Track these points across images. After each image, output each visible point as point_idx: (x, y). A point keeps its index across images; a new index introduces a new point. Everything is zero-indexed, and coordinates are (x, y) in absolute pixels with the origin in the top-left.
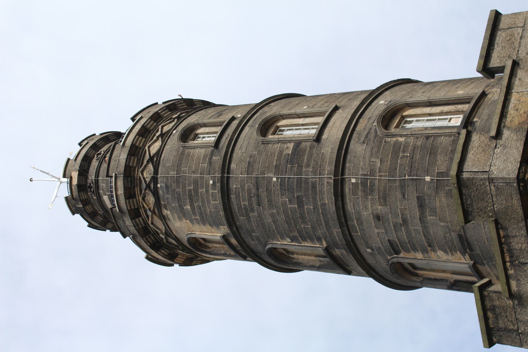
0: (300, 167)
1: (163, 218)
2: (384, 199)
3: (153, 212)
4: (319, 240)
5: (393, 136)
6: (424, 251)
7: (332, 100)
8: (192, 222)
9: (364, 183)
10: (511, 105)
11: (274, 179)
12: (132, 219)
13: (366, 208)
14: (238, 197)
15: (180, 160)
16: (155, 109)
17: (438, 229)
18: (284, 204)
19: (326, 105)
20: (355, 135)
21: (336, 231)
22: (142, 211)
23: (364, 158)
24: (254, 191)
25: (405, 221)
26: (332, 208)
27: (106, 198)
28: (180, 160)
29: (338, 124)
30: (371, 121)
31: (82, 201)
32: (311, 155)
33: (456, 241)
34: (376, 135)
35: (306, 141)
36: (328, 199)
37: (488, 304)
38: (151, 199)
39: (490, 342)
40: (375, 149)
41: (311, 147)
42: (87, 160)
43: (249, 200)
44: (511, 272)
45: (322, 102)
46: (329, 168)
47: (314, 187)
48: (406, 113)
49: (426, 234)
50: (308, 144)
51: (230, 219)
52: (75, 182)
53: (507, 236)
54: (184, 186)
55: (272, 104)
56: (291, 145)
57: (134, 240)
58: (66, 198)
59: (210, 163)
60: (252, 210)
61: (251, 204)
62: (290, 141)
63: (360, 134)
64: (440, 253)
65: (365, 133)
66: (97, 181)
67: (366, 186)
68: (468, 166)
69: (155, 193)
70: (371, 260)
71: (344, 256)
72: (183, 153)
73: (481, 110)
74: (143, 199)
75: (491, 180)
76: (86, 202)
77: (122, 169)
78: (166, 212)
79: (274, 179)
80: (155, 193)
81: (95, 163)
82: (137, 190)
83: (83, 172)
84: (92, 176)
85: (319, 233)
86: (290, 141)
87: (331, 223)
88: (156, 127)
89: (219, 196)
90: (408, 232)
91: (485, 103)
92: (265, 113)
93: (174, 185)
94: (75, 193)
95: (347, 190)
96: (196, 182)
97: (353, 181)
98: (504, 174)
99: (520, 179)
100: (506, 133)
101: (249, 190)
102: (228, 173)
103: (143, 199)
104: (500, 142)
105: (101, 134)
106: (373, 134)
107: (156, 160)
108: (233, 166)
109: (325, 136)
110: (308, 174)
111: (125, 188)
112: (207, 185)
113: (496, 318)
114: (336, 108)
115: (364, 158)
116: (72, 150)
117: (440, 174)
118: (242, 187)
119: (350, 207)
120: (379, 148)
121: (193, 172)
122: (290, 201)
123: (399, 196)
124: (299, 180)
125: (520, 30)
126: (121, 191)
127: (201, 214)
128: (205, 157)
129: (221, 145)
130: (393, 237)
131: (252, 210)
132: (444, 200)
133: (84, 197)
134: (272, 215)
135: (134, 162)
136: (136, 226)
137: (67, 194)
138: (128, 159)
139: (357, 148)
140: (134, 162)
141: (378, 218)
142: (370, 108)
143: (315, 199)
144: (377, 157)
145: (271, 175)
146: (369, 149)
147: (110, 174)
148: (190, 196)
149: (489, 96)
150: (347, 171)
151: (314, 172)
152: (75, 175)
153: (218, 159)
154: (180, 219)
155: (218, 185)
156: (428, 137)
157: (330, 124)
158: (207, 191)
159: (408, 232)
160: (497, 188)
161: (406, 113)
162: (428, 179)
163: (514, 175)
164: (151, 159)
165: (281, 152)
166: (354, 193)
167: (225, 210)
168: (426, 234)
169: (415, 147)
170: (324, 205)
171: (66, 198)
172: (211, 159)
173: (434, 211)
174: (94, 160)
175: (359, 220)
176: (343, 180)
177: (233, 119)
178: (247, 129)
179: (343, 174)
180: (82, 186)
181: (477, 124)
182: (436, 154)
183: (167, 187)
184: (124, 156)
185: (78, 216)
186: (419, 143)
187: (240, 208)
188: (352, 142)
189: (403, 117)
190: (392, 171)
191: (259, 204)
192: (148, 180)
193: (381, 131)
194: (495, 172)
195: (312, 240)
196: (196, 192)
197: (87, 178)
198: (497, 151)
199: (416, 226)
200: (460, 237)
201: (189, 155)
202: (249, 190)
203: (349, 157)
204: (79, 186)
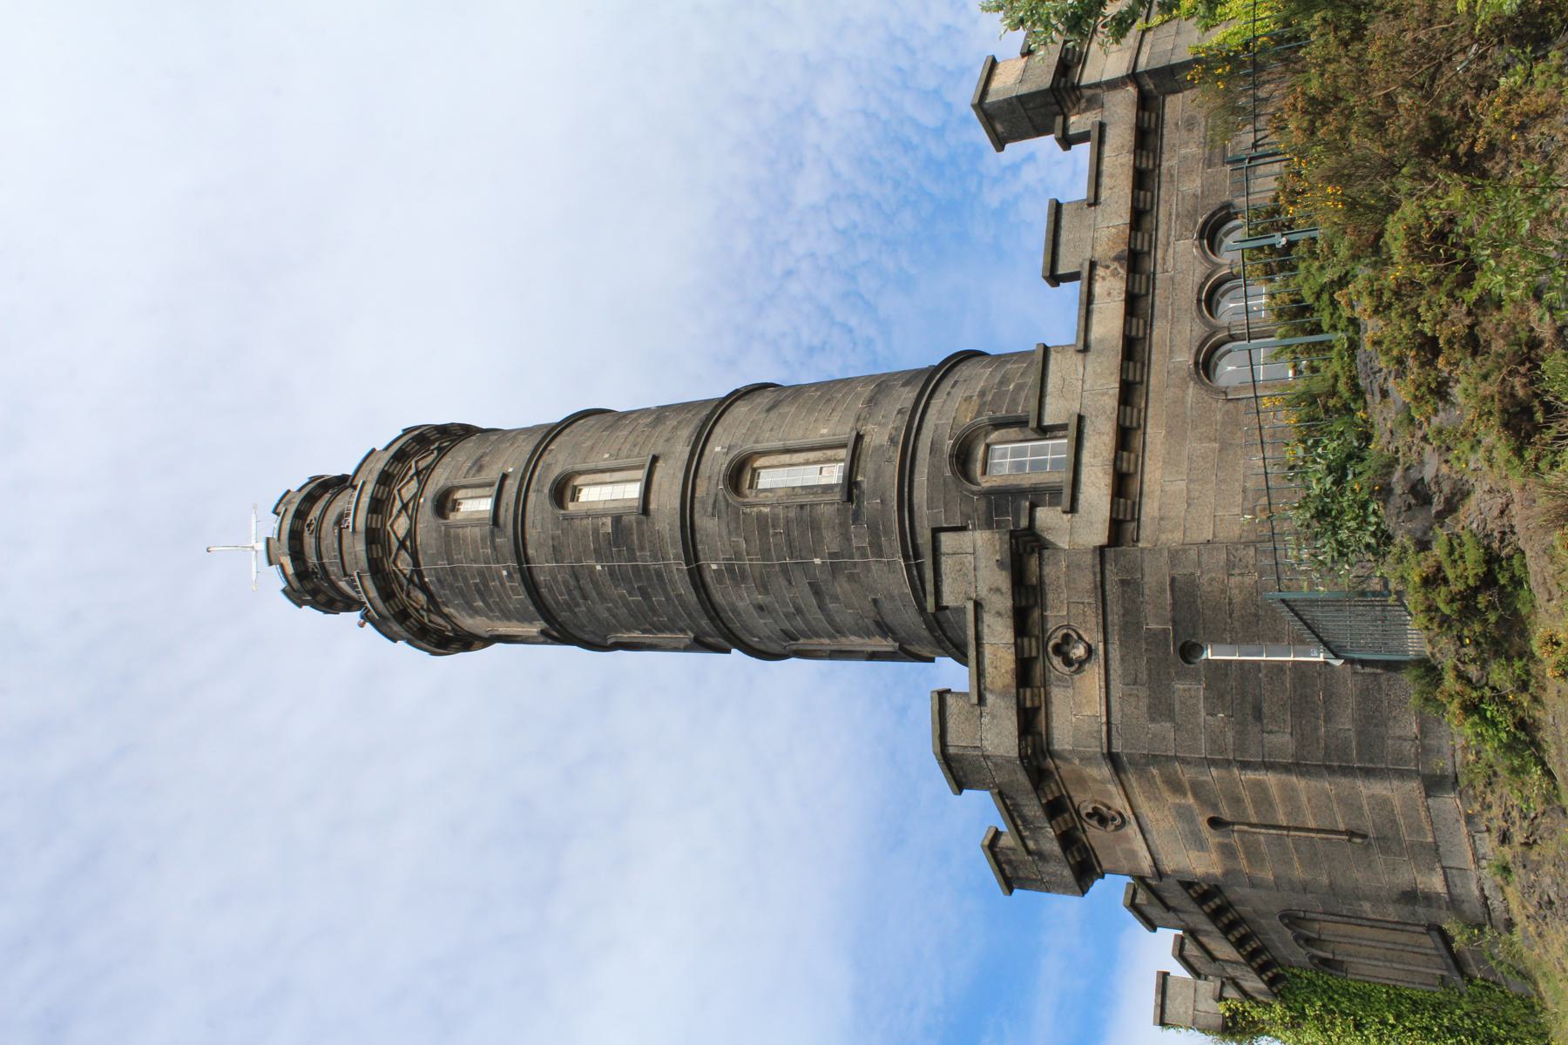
0: (631, 550)
1: (446, 617)
2: (764, 587)
3: (428, 611)
4: (682, 630)
5: (752, 505)
6: (831, 637)
7: (641, 440)
8: (489, 618)
9: (730, 569)
10: (987, 661)
11: (599, 568)
12: (401, 623)
13: (742, 599)
14: (551, 590)
15: (448, 544)
16: (379, 465)
17: (845, 617)
18: (622, 597)
19: (636, 450)
20: (697, 506)
21: (705, 622)
22: (411, 611)
23: (720, 536)
24: (572, 583)
25: (799, 610)
26: (692, 598)
27: (343, 584)
28: (448, 544)
29: (666, 486)
30: (714, 482)
31: (308, 592)
32: (641, 535)
33: (872, 627)
34: (728, 505)
35: (628, 514)
36: (684, 588)
37: (1000, 857)
38: (422, 598)
39: (1010, 890)
40: (733, 525)
41: (639, 523)
42: (295, 537)
43: (569, 592)
44: (1026, 833)
45: (628, 446)
46: (674, 551)
47: (659, 574)
48: (756, 465)
49: (831, 621)
50: (633, 518)
51: (543, 610)
52: (290, 570)
53: (1016, 805)
54: (465, 580)
55: (552, 447)
56: (609, 521)
57: (410, 642)
58: (284, 591)
59: (494, 547)
60: (578, 605)
61: (573, 599)
62: (604, 515)
63: (703, 502)
64: (853, 638)
65: (711, 501)
66: (322, 566)
67: (734, 573)
68: (952, 738)
69: (424, 588)
70: (762, 647)
71: (716, 632)
72: (447, 535)
73: (862, 464)
74: (408, 595)
75: (986, 757)
76: (314, 592)
78: (446, 610)
79: (599, 568)
80: (424, 588)
81: (309, 541)
82: (395, 587)
83: (297, 554)
84: (312, 560)
85: (682, 624)
86: (604, 515)
87: (695, 614)
88: (390, 492)
89: (522, 589)
90: (805, 620)
91: (864, 452)
92: (548, 466)
93: (450, 579)
94: (296, 584)
95: (708, 579)
96: (481, 573)
97: (714, 567)
98: (1001, 751)
99: (1022, 757)
100: (990, 698)
101: (566, 583)
102: (527, 562)
103: (408, 595)
104: (986, 710)
105: (300, 490)
106: (722, 505)
107: (409, 543)
108: (531, 552)
109: (653, 506)
110: (645, 560)
111: (379, 589)
112: (500, 577)
113: (1015, 868)
114: (655, 459)
115: (720, 536)
116: (270, 525)
117: (832, 555)
118: (554, 579)
119: (718, 597)
120: (737, 522)
121: (475, 561)
122: (630, 594)
123: (784, 583)
124: (636, 569)
125: (971, 558)
126: (373, 593)
127: (501, 610)
128: (483, 539)
129: (502, 520)
130: (787, 626)
131: (578, 605)
132: (846, 586)
133: (309, 586)
134: (609, 609)
135: (377, 551)
136: (409, 629)
137: (283, 585)
138: (369, 550)
139: (707, 524)
140: (377, 551)
141: (760, 608)
142: (704, 459)
144: (738, 535)
145: (592, 563)
146: (724, 526)
147: (349, 571)
148: (479, 591)
149: (867, 439)
150: (701, 555)
152: (287, 561)
153: (505, 541)
154: (471, 616)
155: (517, 576)
156: (802, 507)
157: (655, 486)
158: (502, 584)
159: (805, 620)
160: (996, 764)
161: (756, 465)
162: (817, 561)
163: (1014, 753)
164: (402, 545)
165: (596, 531)
166: (720, 582)
167: (535, 604)
168: (831, 621)
169: (788, 521)
170: (679, 596)
171: (284, 591)
172: (493, 541)
173: (835, 598)
174: (306, 534)
175: (735, 610)
176: (699, 568)
177: (505, 477)
178: (532, 496)
179: (697, 559)
180: (303, 573)
181: (865, 486)
182: (819, 529)
183: (439, 580)
184: (360, 547)
185: (307, 608)
186: (792, 514)
187: (557, 603)
188: (696, 516)
189: (754, 470)
190: (765, 553)
191: (585, 598)
192: (407, 572)
193: (733, 499)
194: (990, 749)
195: (672, 631)
196: (486, 585)
197: (305, 562)
198: (985, 720)
199: (815, 615)
200: (877, 623)
201: (457, 537)
202: (566, 583)
203: (698, 536)
204: (298, 574)
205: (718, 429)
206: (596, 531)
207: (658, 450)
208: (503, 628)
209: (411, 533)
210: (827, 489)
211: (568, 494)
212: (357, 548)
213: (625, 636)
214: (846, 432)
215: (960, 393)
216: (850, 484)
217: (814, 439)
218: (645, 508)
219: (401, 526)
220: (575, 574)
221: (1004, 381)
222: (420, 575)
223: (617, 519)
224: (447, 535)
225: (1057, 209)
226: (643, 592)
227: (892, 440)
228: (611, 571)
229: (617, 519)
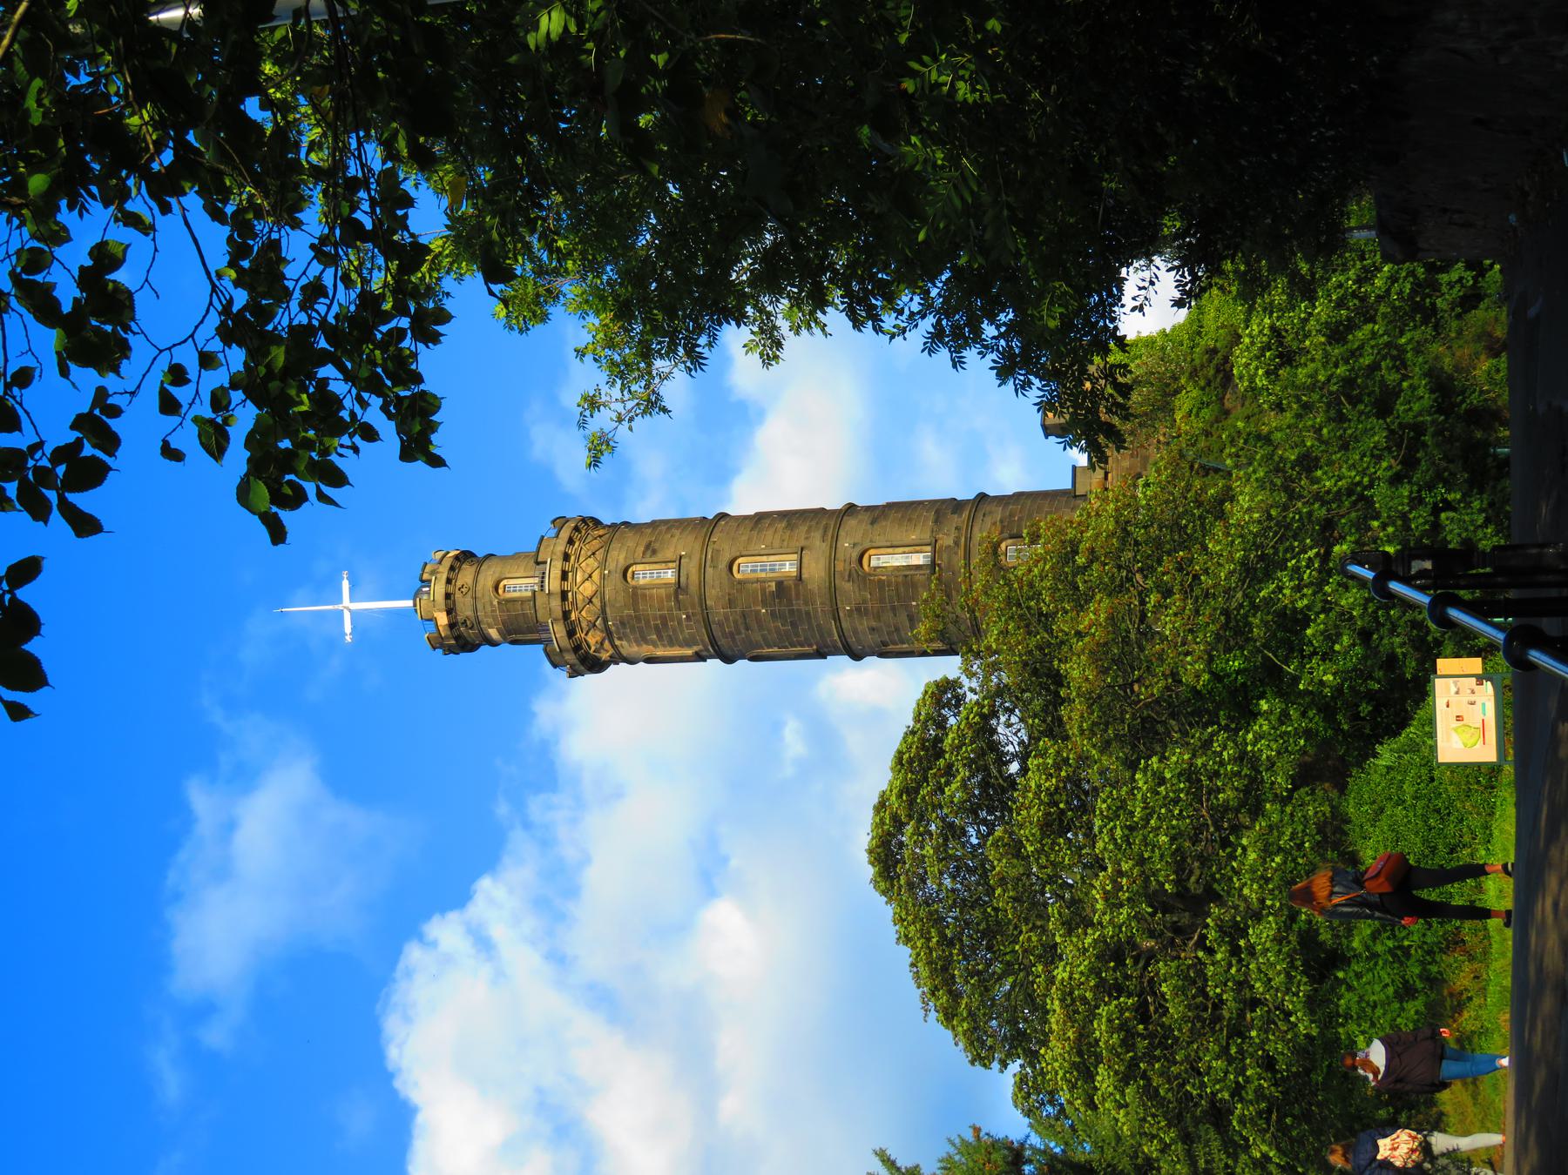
2: (878, 617)
9: (858, 610)
32: (798, 595)
47: (808, 613)
54: (647, 622)
67: (859, 611)
72: (635, 594)
77: (559, 614)
78: (617, 643)
101: (735, 622)
110: (798, 605)
118: (727, 619)
124: (792, 612)
128: (668, 597)
143: (810, 623)
151: (806, 603)
165: (763, 590)
170: (819, 625)
178: (709, 570)
191: (747, 629)
201: (644, 596)
205: (842, 533)
206: (763, 590)
207: (803, 543)
208: (660, 652)
209: (599, 592)
210: (918, 567)
211: (735, 568)
212: (556, 603)
213: (766, 651)
214: (927, 537)
215: (989, 521)
216: (933, 564)
217: (906, 542)
218: (800, 578)
219: (588, 589)
220: (744, 615)
221: (1012, 515)
222: (605, 621)
223: (780, 584)
224: (635, 594)
225: (1074, 468)
226: (793, 624)
227: (957, 543)
228: (773, 614)
229: (780, 584)
